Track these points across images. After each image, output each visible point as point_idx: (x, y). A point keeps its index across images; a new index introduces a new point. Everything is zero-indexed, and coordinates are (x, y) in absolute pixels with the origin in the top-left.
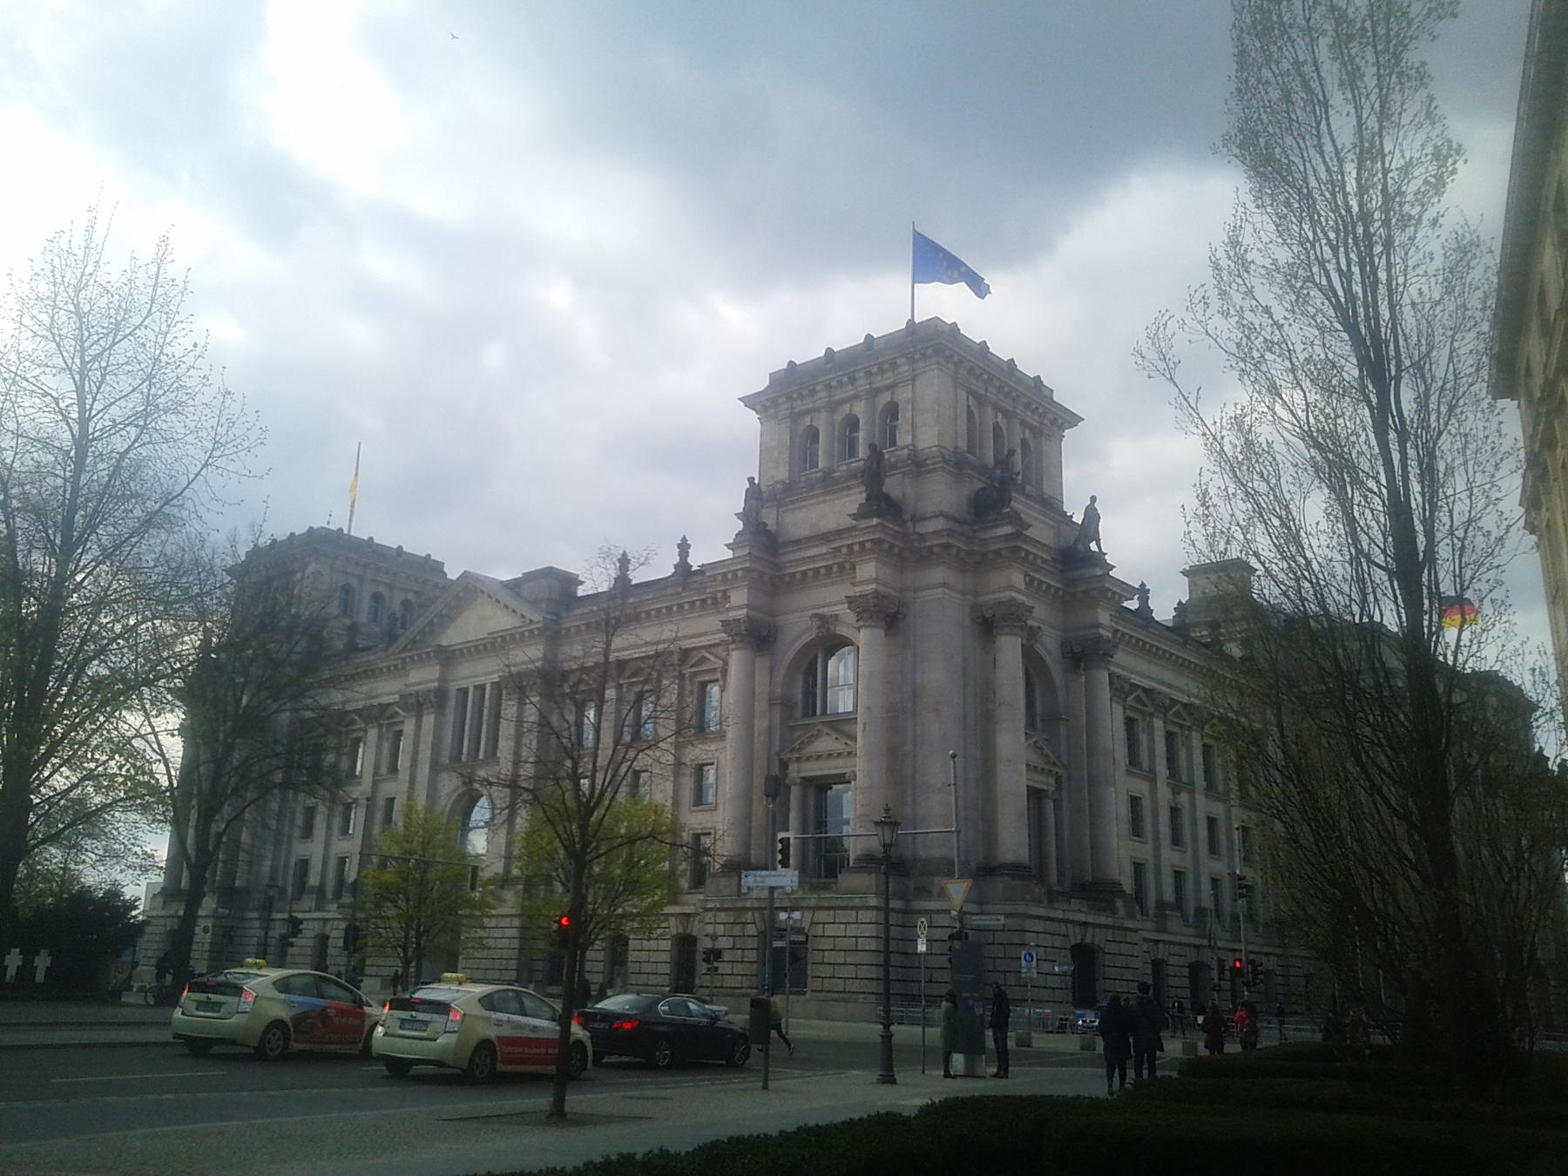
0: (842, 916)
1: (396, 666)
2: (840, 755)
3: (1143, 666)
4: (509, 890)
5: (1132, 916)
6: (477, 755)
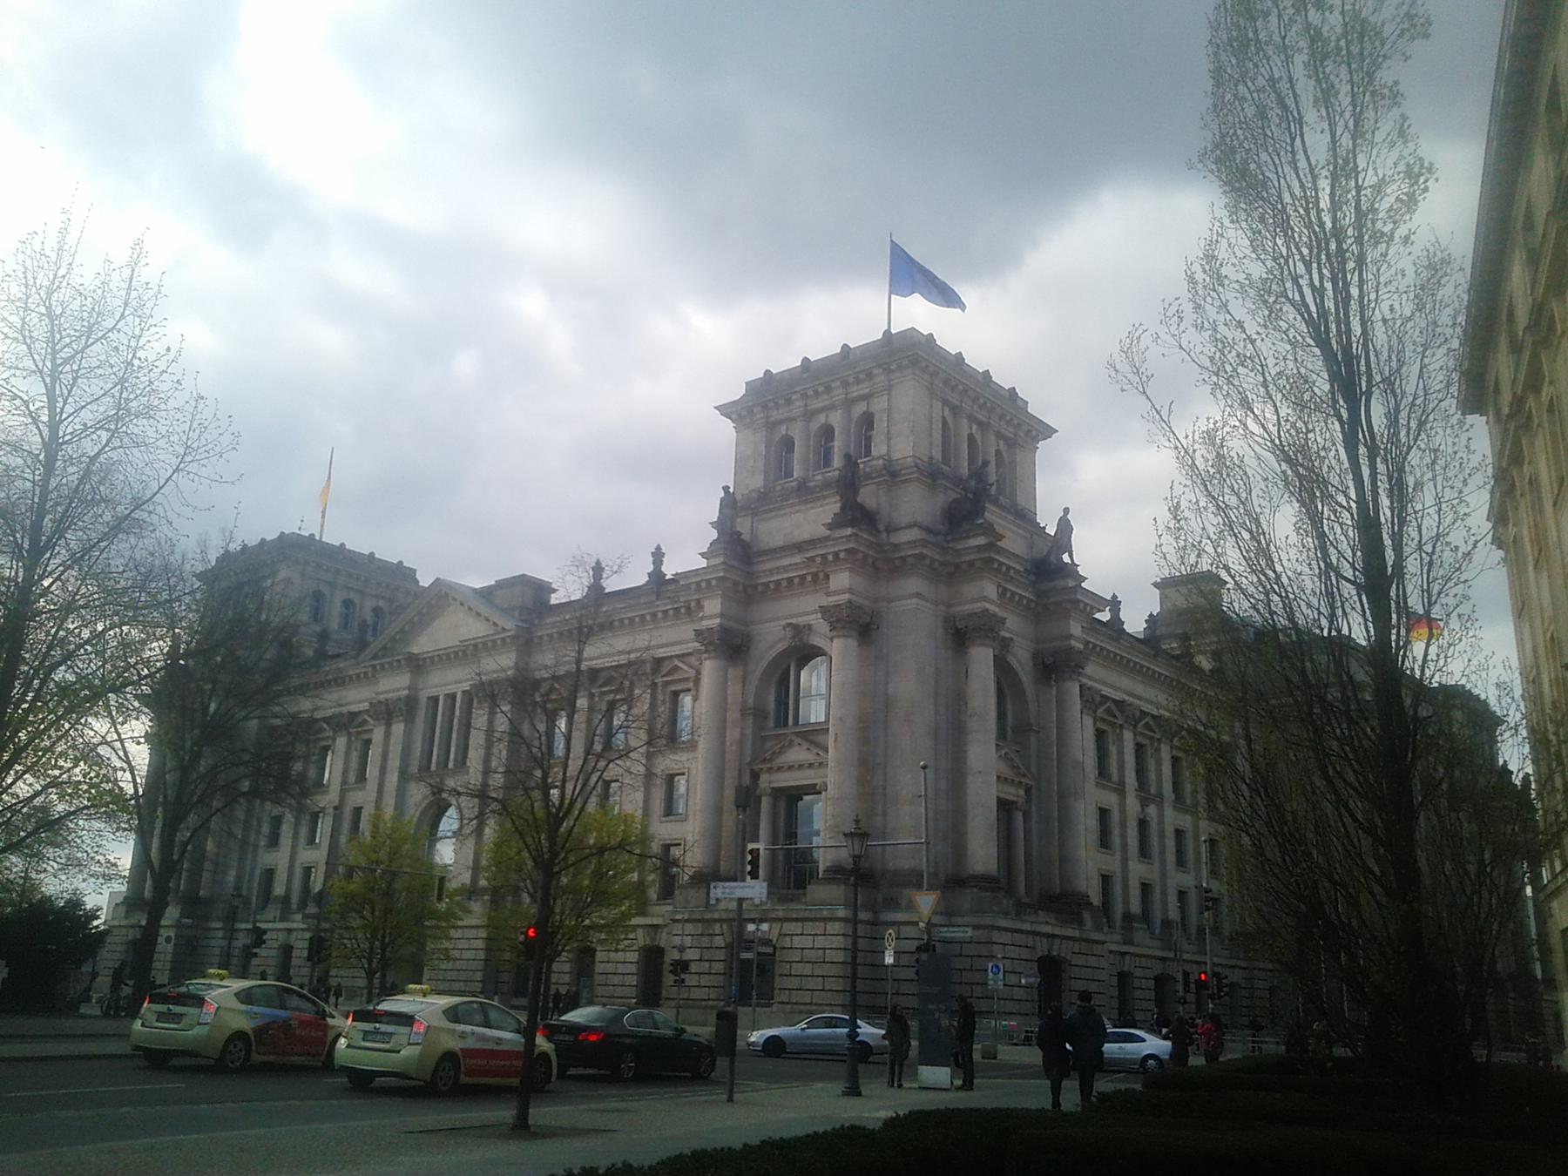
0: (809, 927)
1: (366, 673)
2: (811, 766)
3: (1113, 678)
4: (476, 901)
5: (1098, 929)
6: (446, 766)
